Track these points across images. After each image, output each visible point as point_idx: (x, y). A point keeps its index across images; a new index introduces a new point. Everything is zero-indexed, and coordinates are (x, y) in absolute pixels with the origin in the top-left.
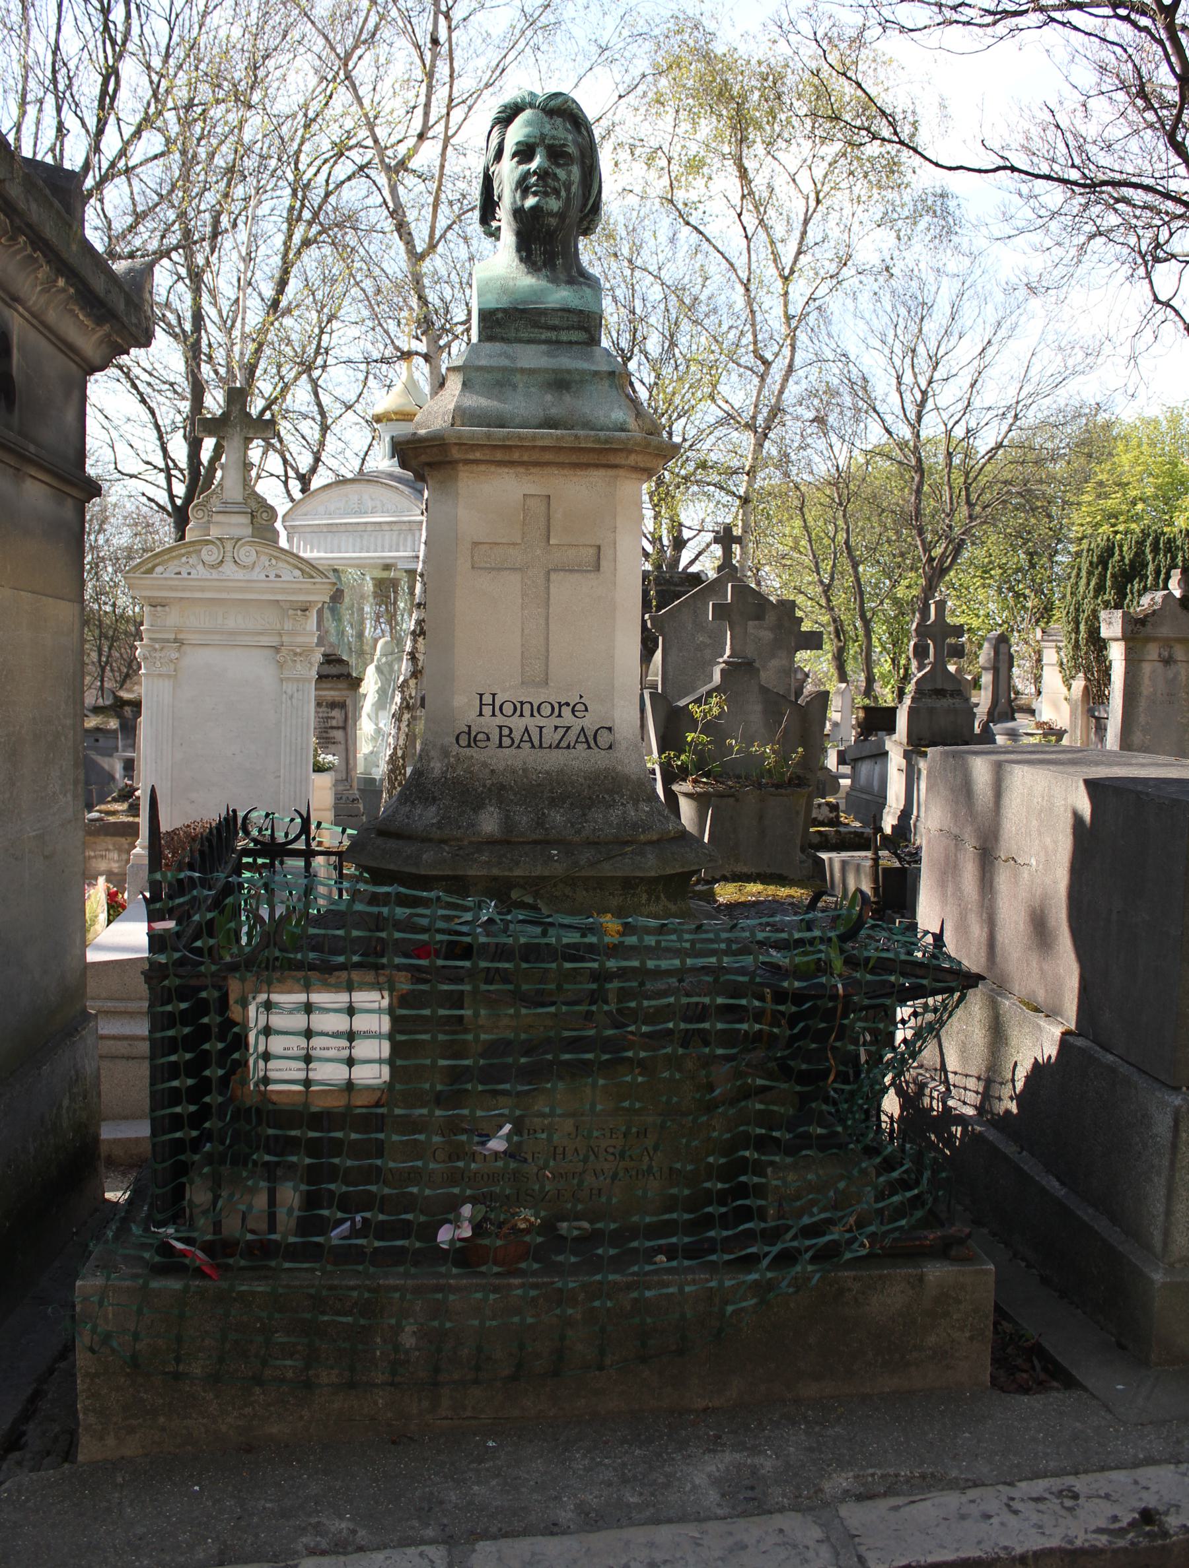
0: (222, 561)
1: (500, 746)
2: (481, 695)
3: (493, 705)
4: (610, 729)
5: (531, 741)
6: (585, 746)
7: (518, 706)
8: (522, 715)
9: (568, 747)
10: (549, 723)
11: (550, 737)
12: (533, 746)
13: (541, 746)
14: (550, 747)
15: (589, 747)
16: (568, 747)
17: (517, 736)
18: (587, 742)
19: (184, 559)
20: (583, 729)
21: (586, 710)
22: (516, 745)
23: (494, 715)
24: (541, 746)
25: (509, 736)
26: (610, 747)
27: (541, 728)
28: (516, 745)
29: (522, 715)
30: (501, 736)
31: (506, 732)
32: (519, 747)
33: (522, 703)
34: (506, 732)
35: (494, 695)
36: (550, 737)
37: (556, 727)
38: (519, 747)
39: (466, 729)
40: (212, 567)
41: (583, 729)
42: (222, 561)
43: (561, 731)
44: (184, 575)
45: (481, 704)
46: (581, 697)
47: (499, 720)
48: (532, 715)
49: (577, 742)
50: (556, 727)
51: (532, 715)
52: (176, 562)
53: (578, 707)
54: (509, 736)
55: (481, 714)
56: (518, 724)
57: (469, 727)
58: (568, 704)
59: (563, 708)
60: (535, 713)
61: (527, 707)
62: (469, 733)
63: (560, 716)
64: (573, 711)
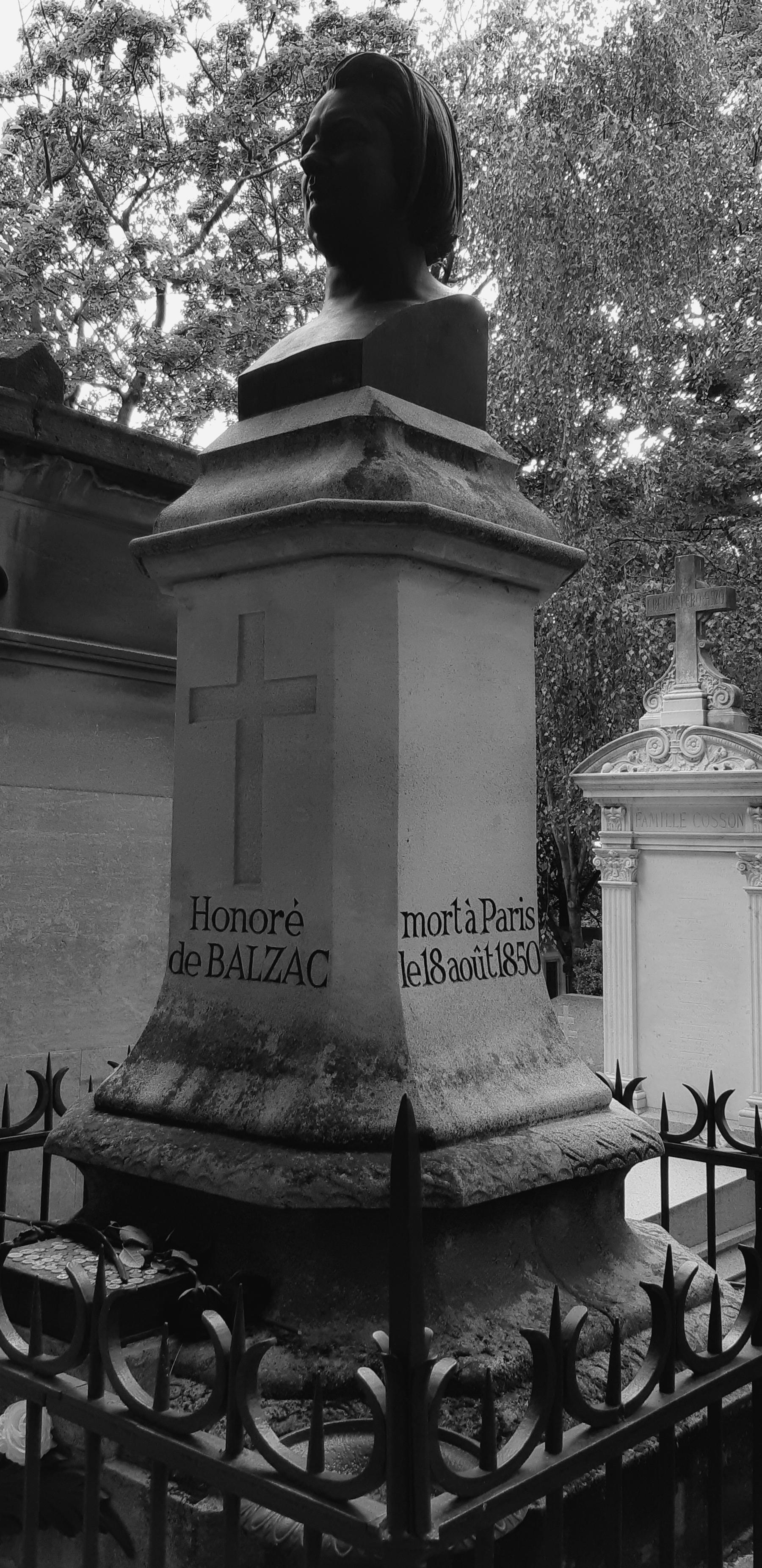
0: (668, 756)
1: (209, 974)
2: (195, 898)
3: (206, 913)
4: (326, 954)
5: (240, 968)
6: (296, 978)
7: (231, 913)
8: (233, 930)
9: (278, 981)
10: (262, 941)
11: (262, 963)
12: (242, 977)
13: (250, 978)
14: (259, 979)
15: (301, 983)
16: (278, 981)
17: (227, 959)
18: (299, 973)
19: (631, 753)
20: (296, 954)
21: (301, 924)
22: (224, 974)
23: (206, 928)
24: (250, 978)
25: (219, 959)
26: (324, 984)
27: (252, 948)
28: (224, 974)
29: (233, 930)
30: (212, 959)
31: (216, 954)
32: (227, 977)
33: (235, 911)
34: (216, 954)
35: (207, 898)
36: (262, 963)
37: (268, 949)
38: (227, 977)
39: (179, 949)
40: (660, 762)
41: (296, 954)
42: (668, 756)
43: (273, 954)
44: (631, 772)
45: (195, 913)
46: (296, 903)
47: (212, 936)
48: (244, 930)
49: (288, 972)
50: (268, 949)
51: (244, 930)
52: (623, 759)
53: (294, 919)
54: (219, 959)
55: (194, 928)
56: (229, 941)
57: (183, 944)
58: (281, 914)
59: (278, 920)
60: (248, 927)
61: (239, 915)
62: (182, 954)
63: (272, 932)
64: (287, 924)
